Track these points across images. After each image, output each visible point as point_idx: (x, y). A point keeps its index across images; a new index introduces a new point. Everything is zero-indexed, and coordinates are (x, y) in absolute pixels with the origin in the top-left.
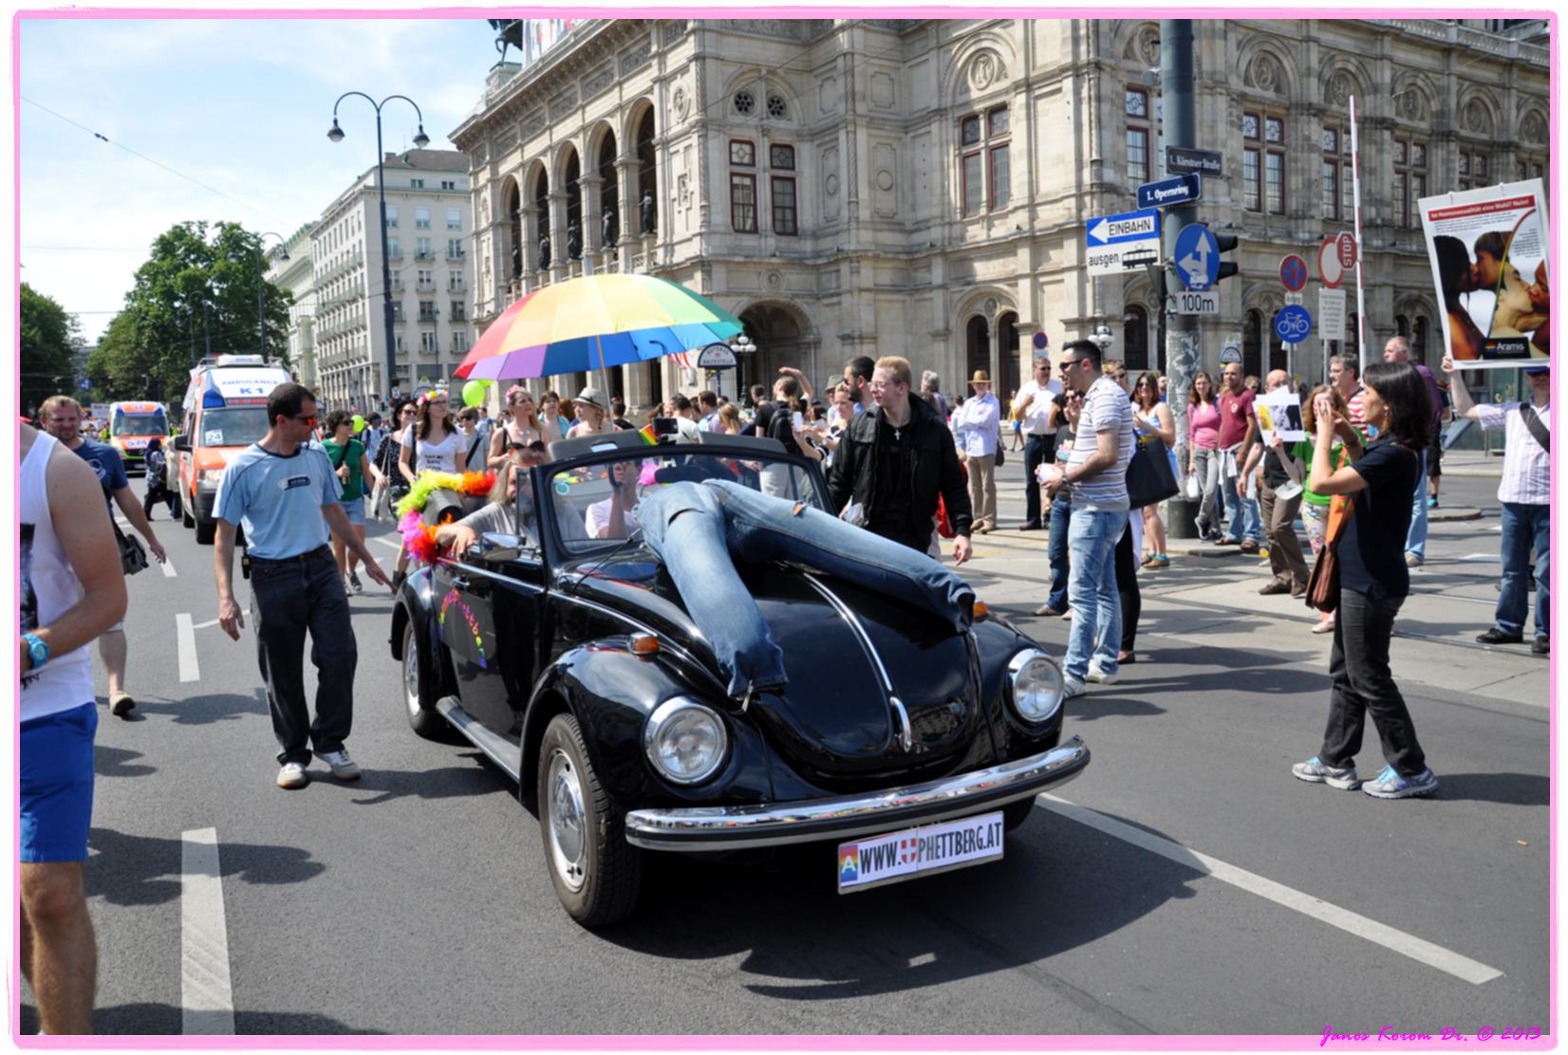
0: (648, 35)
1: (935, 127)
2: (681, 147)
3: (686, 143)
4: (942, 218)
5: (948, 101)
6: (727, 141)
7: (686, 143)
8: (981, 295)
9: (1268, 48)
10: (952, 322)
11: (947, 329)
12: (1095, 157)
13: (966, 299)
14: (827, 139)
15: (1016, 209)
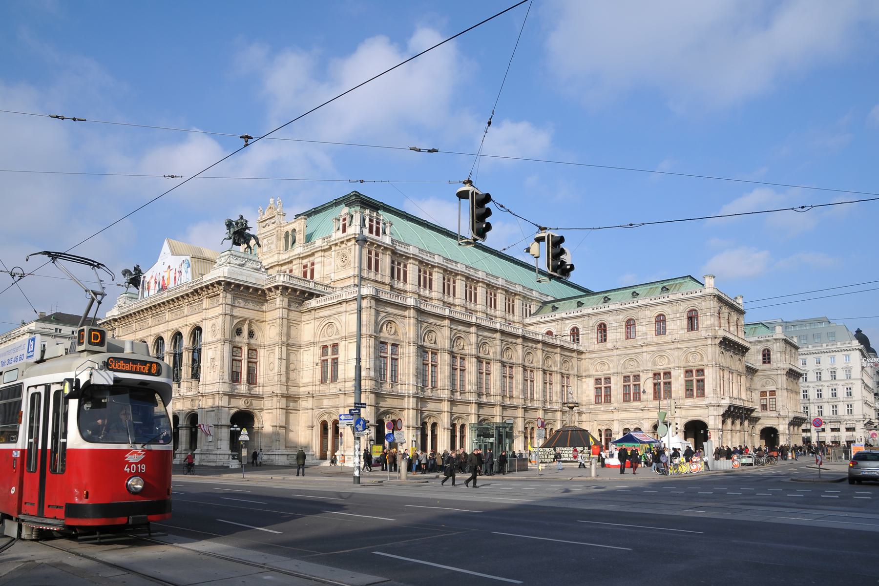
0: (202, 300)
1: (312, 348)
2: (213, 347)
3: (215, 346)
4: (313, 383)
5: (317, 340)
6: (232, 346)
7: (215, 346)
8: (326, 413)
9: (432, 329)
10: (315, 424)
11: (313, 424)
12: (368, 367)
13: (320, 414)
14: (271, 349)
15: (339, 382)
